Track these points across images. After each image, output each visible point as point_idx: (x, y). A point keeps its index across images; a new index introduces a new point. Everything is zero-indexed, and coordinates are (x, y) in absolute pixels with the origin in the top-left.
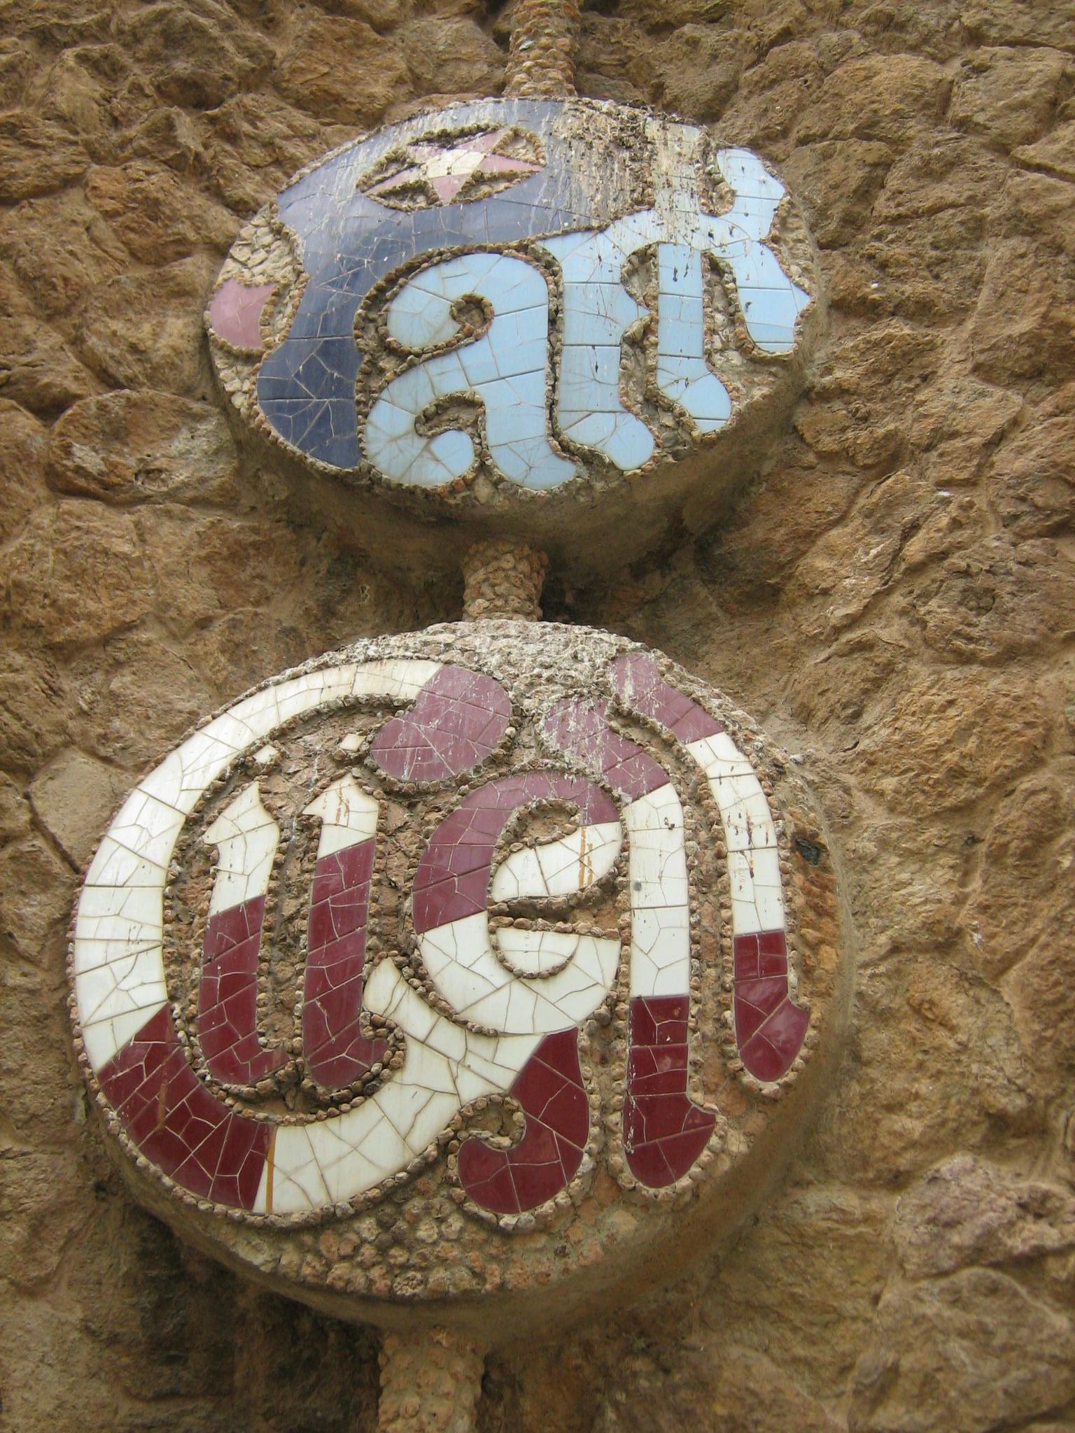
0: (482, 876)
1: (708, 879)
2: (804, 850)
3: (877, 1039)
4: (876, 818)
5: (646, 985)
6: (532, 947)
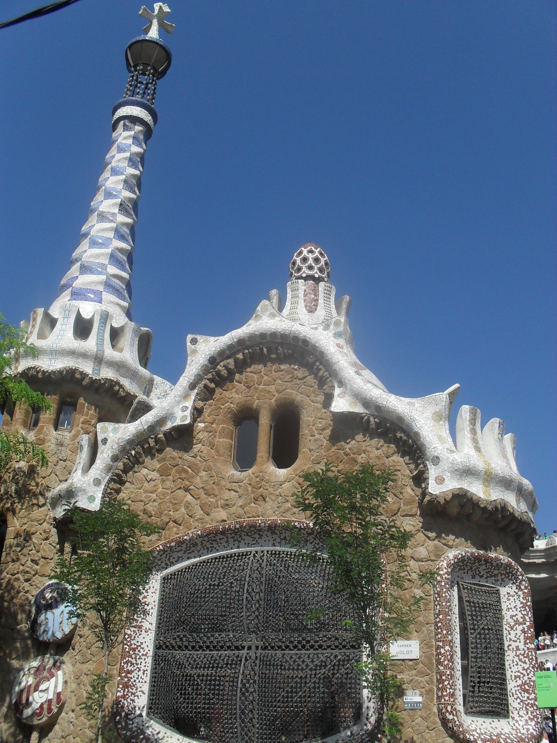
0: (38, 688)
1: (56, 687)
2: (66, 682)
3: (69, 700)
4: (73, 678)
5: (49, 698)
6: (41, 694)
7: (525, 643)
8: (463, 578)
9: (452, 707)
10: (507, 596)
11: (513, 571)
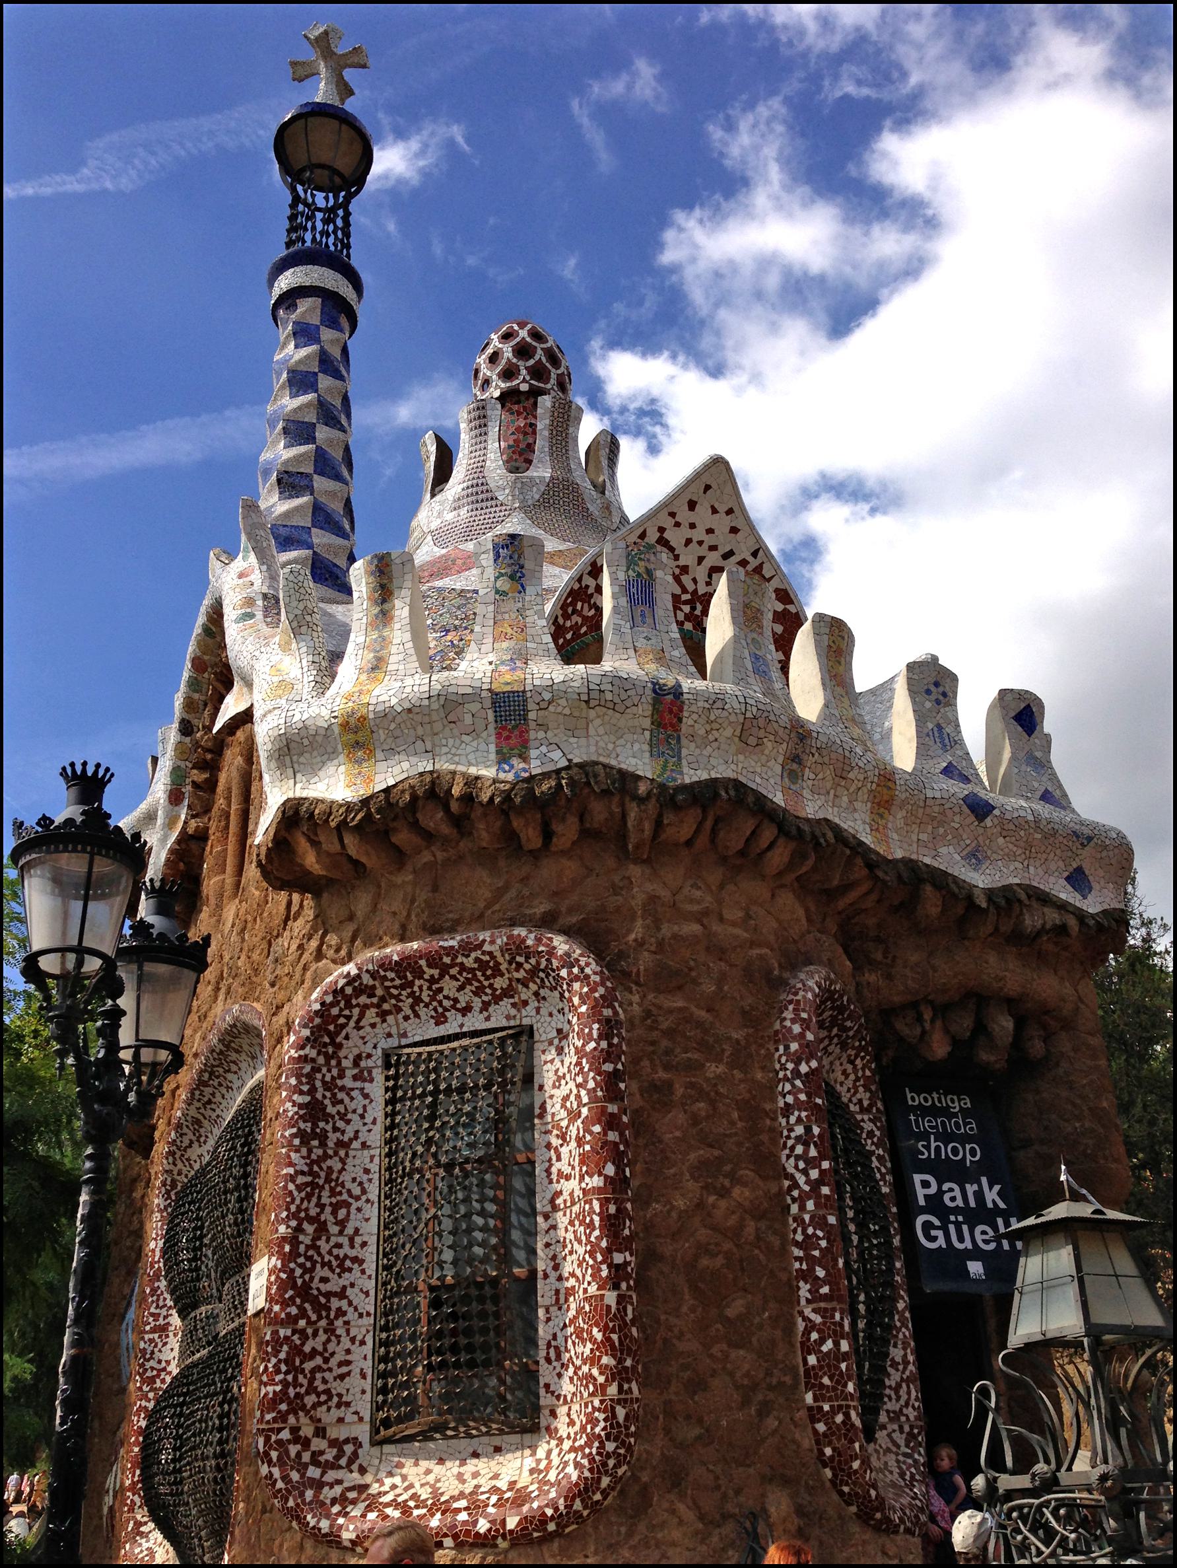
7: (582, 1178)
8: (405, 1035)
9: (267, 1439)
10: (556, 1041)
11: (538, 963)
